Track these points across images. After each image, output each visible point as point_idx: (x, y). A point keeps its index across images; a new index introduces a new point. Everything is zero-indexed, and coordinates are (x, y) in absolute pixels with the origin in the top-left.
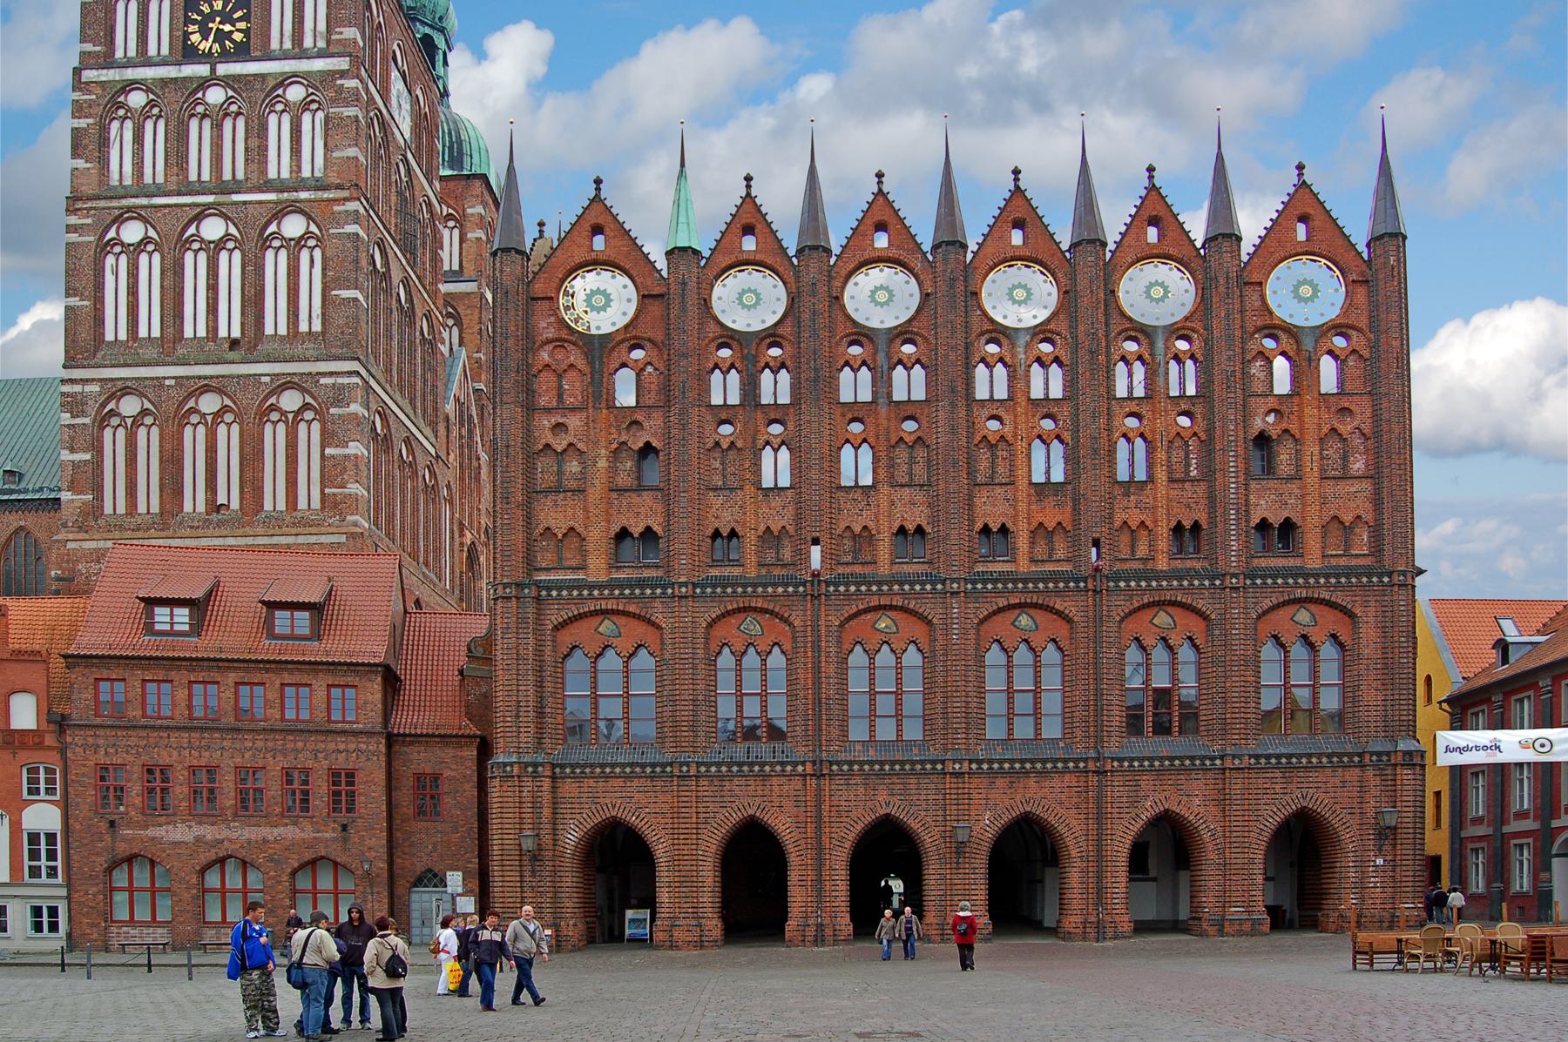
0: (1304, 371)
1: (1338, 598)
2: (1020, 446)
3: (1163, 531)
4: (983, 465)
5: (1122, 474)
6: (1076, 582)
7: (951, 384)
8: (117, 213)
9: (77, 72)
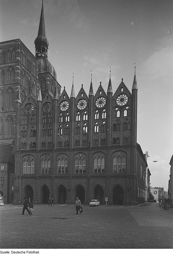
0: (122, 113)
1: (124, 150)
3: (99, 140)
6: (88, 148)
7: (73, 119)
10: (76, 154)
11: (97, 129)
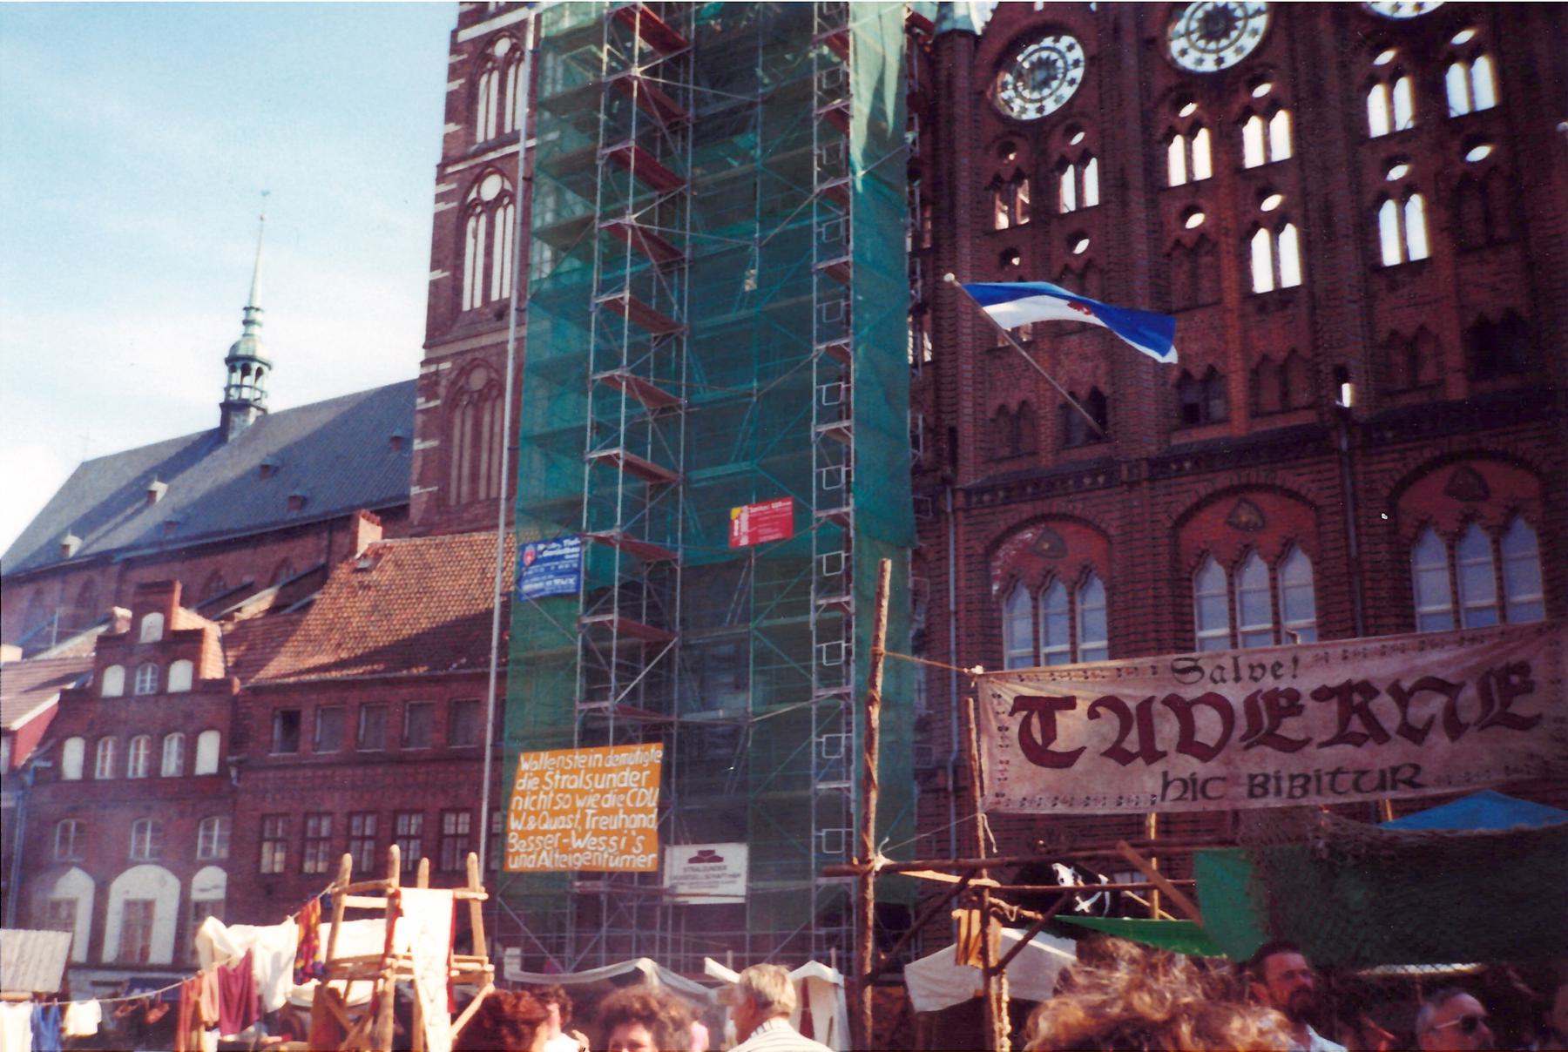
2: (1228, 244)
4: (1180, 278)
5: (1391, 256)
7: (1135, 175)
8: (478, 170)
9: (454, 34)
10: (1198, 507)
11: (1405, 232)
